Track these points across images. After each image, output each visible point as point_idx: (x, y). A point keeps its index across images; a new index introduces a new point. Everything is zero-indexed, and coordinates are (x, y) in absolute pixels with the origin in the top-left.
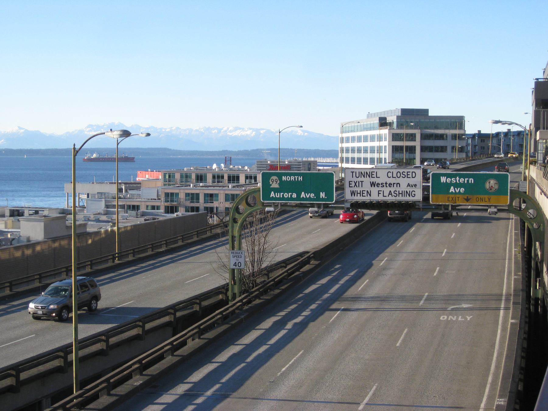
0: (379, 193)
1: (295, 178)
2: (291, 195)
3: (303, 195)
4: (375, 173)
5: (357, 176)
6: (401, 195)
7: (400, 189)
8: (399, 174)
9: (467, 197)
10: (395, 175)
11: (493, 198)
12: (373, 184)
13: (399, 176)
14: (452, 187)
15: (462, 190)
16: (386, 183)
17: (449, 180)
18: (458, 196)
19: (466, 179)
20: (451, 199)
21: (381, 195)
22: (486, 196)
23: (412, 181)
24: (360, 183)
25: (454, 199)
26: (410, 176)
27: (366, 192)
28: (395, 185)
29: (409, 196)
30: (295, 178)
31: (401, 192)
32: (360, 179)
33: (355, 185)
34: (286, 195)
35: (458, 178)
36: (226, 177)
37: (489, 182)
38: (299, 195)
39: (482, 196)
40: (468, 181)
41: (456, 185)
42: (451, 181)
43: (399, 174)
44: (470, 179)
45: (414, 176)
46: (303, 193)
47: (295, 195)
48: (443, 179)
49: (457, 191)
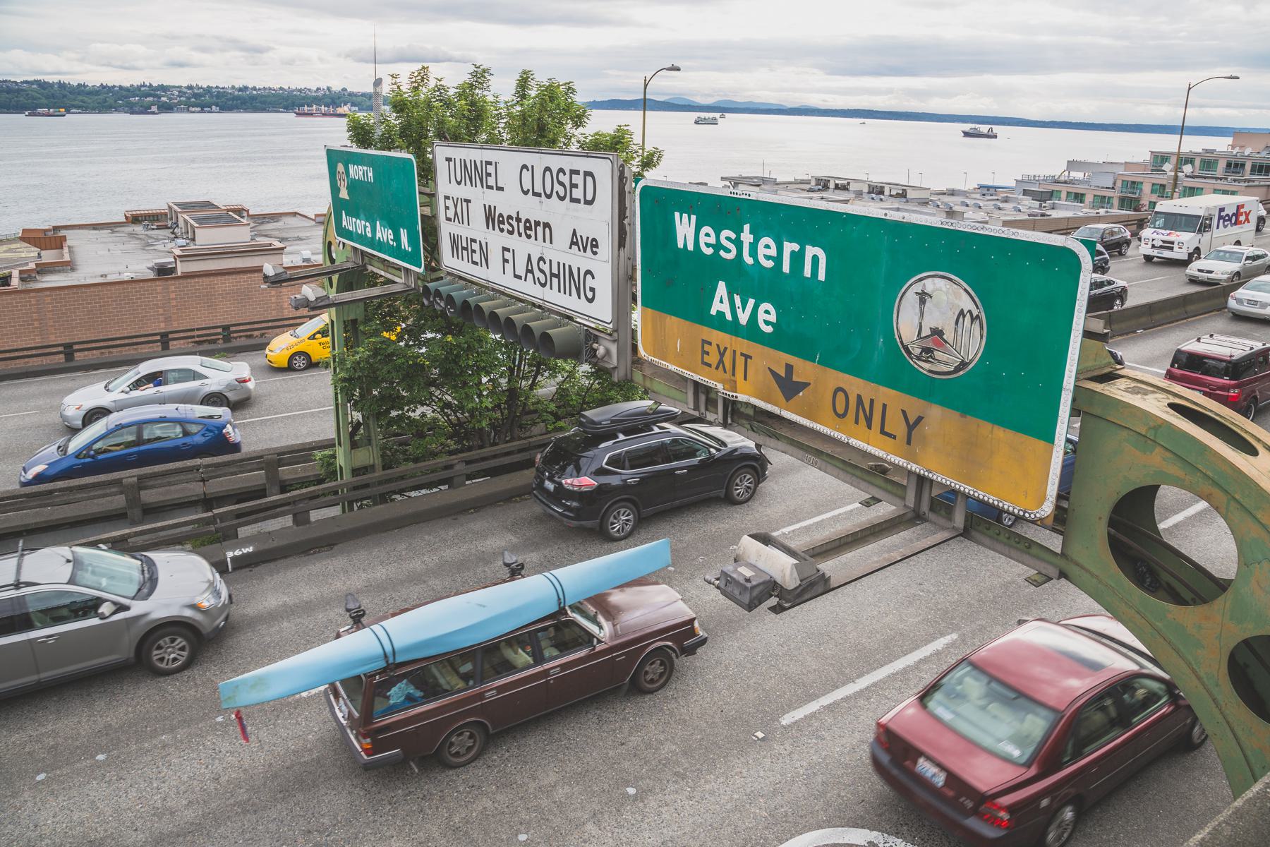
14: (722, 288)
16: (519, 220)
25: (727, 359)
27: (476, 246)
35: (747, 237)
40: (797, 258)
42: (718, 246)
44: (811, 251)
48: (684, 229)
49: (744, 318)
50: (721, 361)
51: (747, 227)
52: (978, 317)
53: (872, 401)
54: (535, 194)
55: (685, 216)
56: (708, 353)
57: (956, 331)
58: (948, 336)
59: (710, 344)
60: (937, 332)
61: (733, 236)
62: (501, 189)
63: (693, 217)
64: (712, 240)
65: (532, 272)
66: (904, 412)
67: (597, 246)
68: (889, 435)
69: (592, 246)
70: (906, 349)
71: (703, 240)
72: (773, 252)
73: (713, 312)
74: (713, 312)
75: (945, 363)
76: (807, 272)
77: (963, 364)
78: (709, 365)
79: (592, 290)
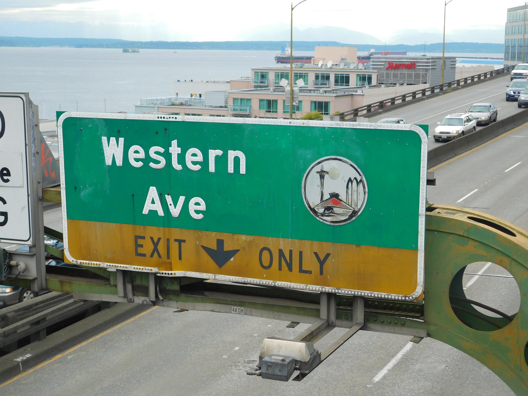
9: (220, 243)
11: (344, 257)
14: (153, 192)
15: (197, 206)
17: (136, 153)
18: (176, 233)
19: (213, 154)
20: (147, 247)
22: (309, 248)
25: (161, 247)
35: (175, 149)
36: (332, 79)
40: (221, 161)
41: (172, 182)
42: (147, 159)
44: (232, 154)
48: (113, 150)
49: (175, 211)
50: (156, 249)
51: (174, 143)
52: (361, 181)
53: (291, 251)
55: (113, 140)
56: (141, 246)
57: (347, 192)
58: (343, 196)
59: (143, 238)
60: (335, 196)
61: (162, 150)
63: (121, 140)
64: (142, 155)
66: (316, 254)
67: (9, 174)
70: (313, 210)
71: (132, 156)
72: (200, 158)
73: (145, 211)
74: (145, 211)
75: (342, 215)
76: (231, 169)
77: (354, 213)
78: (144, 255)
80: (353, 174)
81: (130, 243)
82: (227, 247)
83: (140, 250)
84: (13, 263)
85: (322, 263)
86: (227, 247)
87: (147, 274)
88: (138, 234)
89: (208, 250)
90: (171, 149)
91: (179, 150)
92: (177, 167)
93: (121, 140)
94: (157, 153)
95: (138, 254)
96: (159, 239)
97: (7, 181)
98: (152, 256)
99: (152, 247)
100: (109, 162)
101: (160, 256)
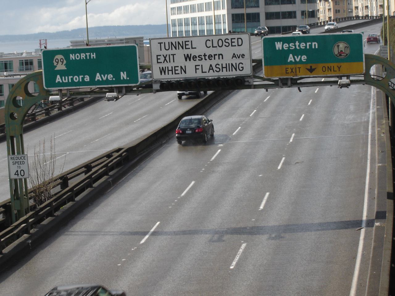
0: (196, 69)
1: (86, 56)
2: (83, 78)
3: (98, 77)
4: (189, 43)
5: (167, 48)
6: (224, 69)
7: (224, 62)
8: (220, 41)
9: (311, 67)
10: (215, 44)
12: (187, 57)
13: (220, 45)
14: (291, 56)
15: (304, 58)
16: (205, 55)
17: (286, 46)
18: (299, 66)
19: (308, 44)
20: (290, 71)
21: (199, 71)
22: (335, 65)
23: (238, 50)
24: (171, 57)
26: (236, 44)
27: (179, 69)
28: (217, 57)
29: (236, 70)
30: (86, 56)
31: (224, 66)
32: (170, 52)
33: (165, 59)
34: (76, 79)
35: (297, 44)
37: (338, 46)
38: (93, 77)
39: (330, 65)
40: (311, 46)
41: (296, 52)
42: (289, 47)
43: (220, 41)
44: (313, 44)
45: (240, 44)
46: (98, 74)
47: (87, 78)
49: (298, 60)
50: (292, 71)
51: (297, 42)
52: (348, 47)
54: (213, 47)
56: (288, 71)
59: (288, 68)
60: (342, 51)
61: (293, 44)
62: (196, 48)
63: (281, 43)
64: (288, 46)
65: (212, 69)
66: (338, 66)
67: (244, 56)
68: (335, 71)
69: (242, 56)
72: (305, 45)
74: (289, 61)
75: (343, 56)
76: (313, 47)
77: (347, 55)
78: (288, 73)
79: (243, 67)
80: (346, 45)
81: (284, 71)
82: (313, 68)
83: (287, 72)
84: (246, 80)
85: (339, 68)
86: (313, 68)
87: (287, 79)
88: (286, 67)
89: (308, 69)
90: (296, 44)
91: (299, 44)
92: (299, 48)
93: (281, 43)
94: (292, 45)
95: (286, 73)
96: (293, 68)
97: (244, 58)
98: (291, 73)
99: (291, 70)
100: (277, 49)
101: (293, 73)
